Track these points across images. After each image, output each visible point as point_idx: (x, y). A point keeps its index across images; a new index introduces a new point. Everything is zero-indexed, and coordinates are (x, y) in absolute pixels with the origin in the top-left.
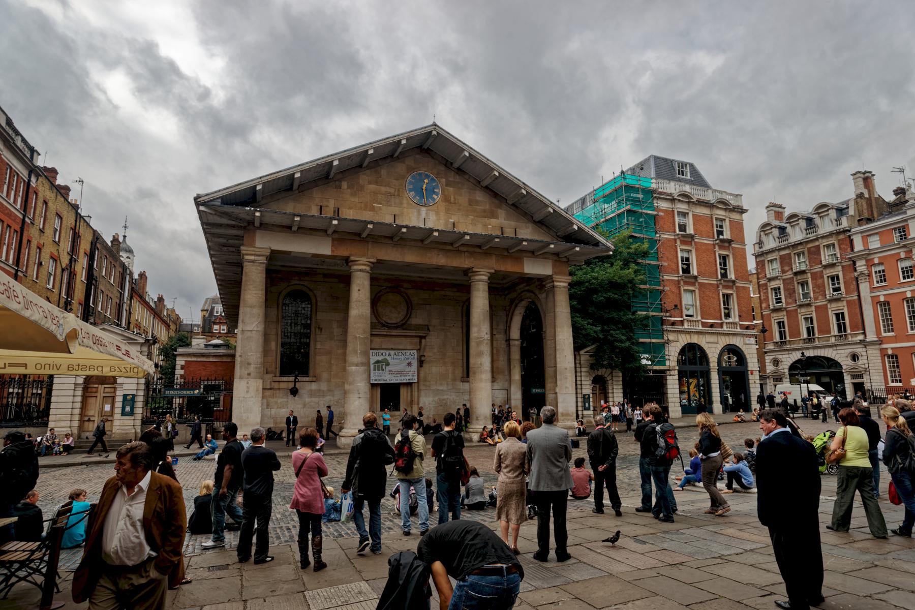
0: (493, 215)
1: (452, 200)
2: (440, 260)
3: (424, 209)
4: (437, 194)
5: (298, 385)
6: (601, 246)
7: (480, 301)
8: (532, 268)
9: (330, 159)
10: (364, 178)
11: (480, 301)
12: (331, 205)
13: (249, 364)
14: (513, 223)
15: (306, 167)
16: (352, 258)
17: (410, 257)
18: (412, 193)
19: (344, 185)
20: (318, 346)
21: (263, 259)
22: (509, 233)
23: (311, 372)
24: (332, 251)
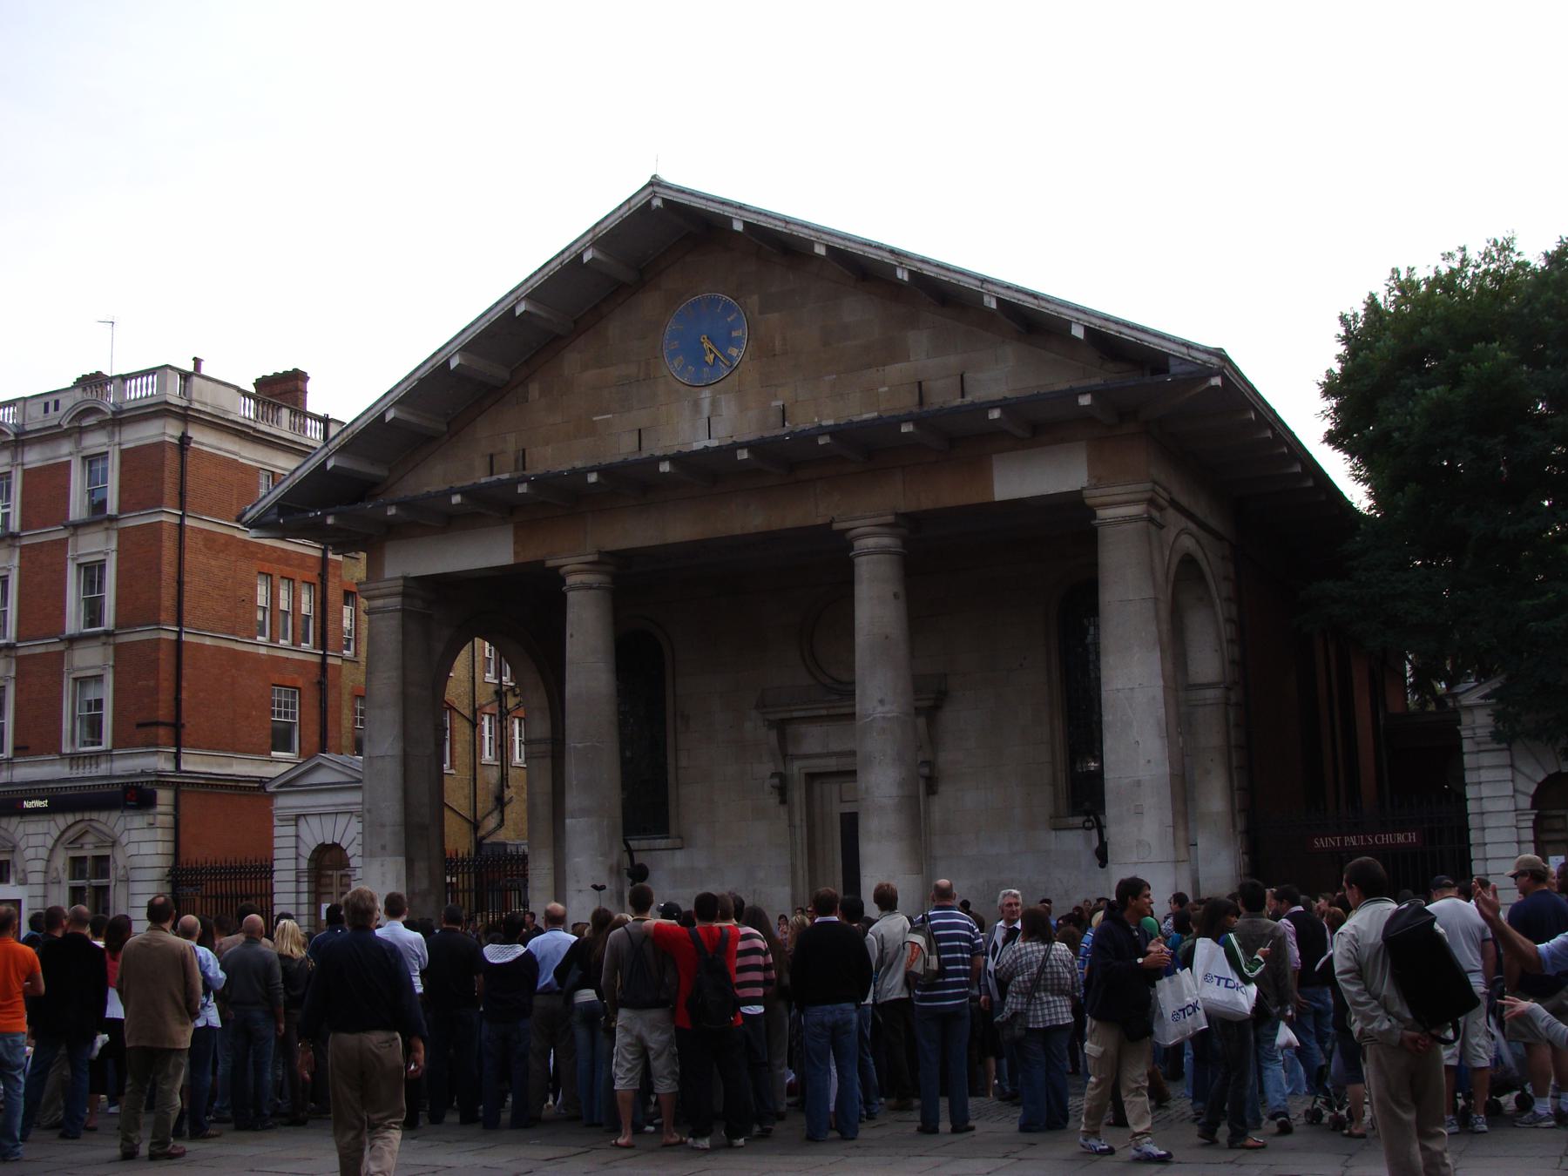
0: (891, 352)
1: (778, 343)
2: (749, 518)
3: (706, 394)
4: (735, 342)
6: (1175, 368)
7: (875, 605)
8: (1020, 480)
9: (440, 359)
10: (572, 361)
11: (875, 605)
12: (511, 445)
13: (383, 826)
14: (953, 360)
15: (401, 392)
16: (550, 563)
17: (677, 528)
18: (678, 362)
19: (534, 390)
21: (395, 602)
22: (943, 396)
24: (516, 554)
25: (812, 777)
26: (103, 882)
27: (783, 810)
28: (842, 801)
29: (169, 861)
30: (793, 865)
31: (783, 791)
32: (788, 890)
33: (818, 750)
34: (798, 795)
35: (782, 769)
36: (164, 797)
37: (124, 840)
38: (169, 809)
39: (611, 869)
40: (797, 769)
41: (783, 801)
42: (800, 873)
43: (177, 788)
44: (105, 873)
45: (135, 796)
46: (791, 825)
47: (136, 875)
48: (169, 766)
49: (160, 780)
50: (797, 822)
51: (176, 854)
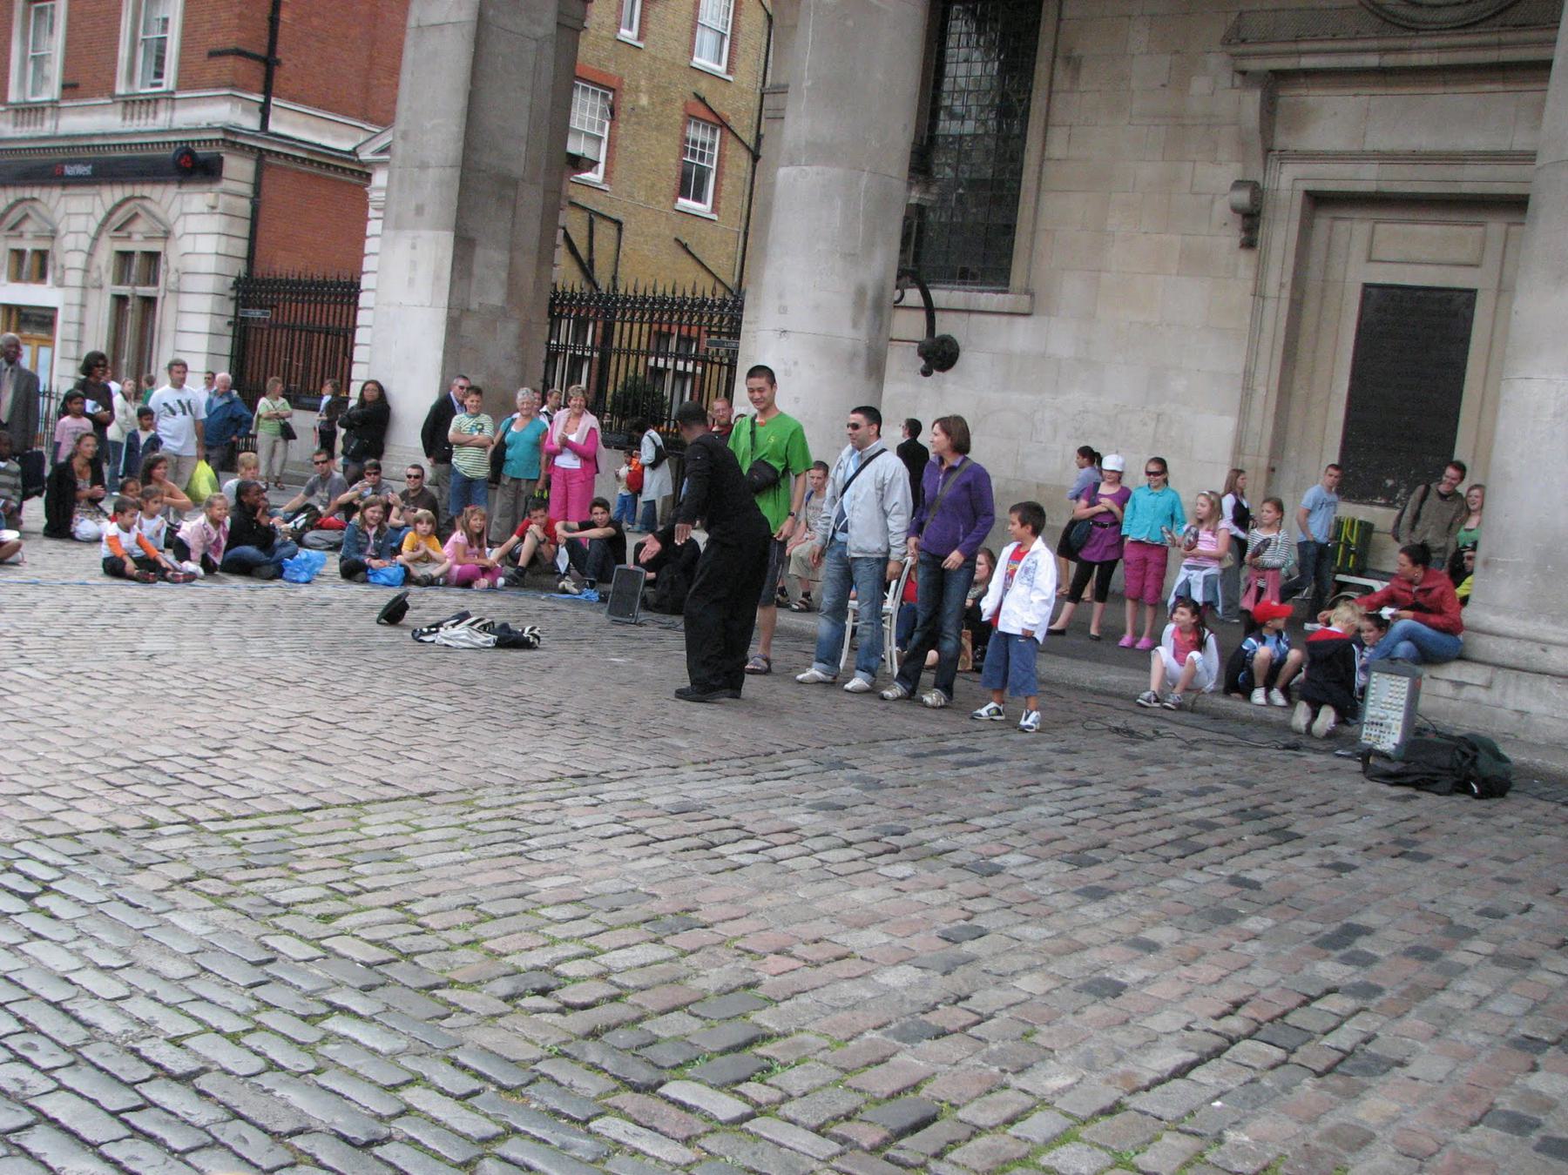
5: (945, 325)
20: (1056, 149)
23: (1017, 278)
25: (1318, 200)
26: (148, 291)
27: (1246, 259)
28: (1370, 260)
29: (240, 268)
30: (1248, 374)
31: (1251, 220)
32: (1228, 424)
33: (1338, 143)
34: (1281, 234)
35: (1256, 174)
36: (239, 169)
37: (178, 230)
38: (247, 189)
39: (861, 292)
40: (1288, 182)
41: (1249, 244)
42: (1261, 391)
43: (260, 157)
44: (152, 279)
45: (193, 165)
46: (1258, 294)
47: (189, 283)
48: (251, 123)
49: (231, 138)
50: (1272, 287)
51: (250, 259)
